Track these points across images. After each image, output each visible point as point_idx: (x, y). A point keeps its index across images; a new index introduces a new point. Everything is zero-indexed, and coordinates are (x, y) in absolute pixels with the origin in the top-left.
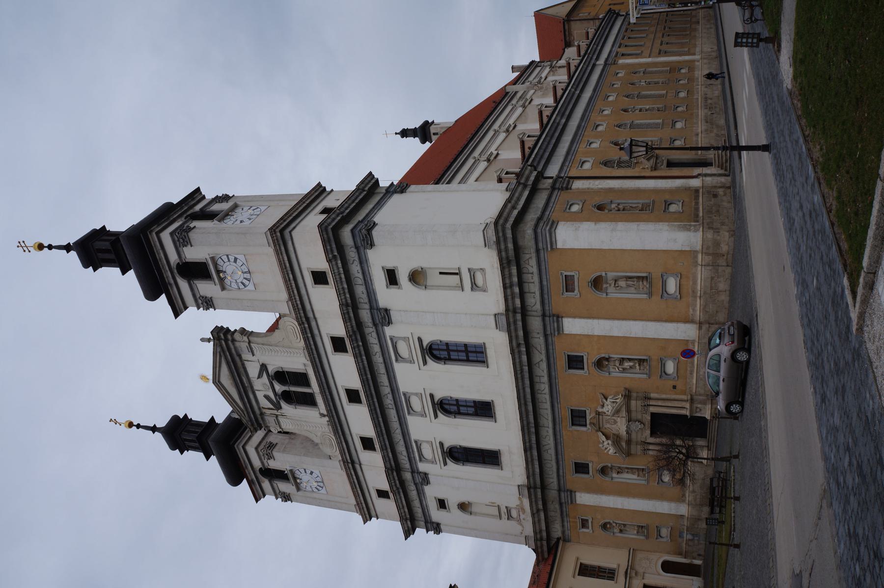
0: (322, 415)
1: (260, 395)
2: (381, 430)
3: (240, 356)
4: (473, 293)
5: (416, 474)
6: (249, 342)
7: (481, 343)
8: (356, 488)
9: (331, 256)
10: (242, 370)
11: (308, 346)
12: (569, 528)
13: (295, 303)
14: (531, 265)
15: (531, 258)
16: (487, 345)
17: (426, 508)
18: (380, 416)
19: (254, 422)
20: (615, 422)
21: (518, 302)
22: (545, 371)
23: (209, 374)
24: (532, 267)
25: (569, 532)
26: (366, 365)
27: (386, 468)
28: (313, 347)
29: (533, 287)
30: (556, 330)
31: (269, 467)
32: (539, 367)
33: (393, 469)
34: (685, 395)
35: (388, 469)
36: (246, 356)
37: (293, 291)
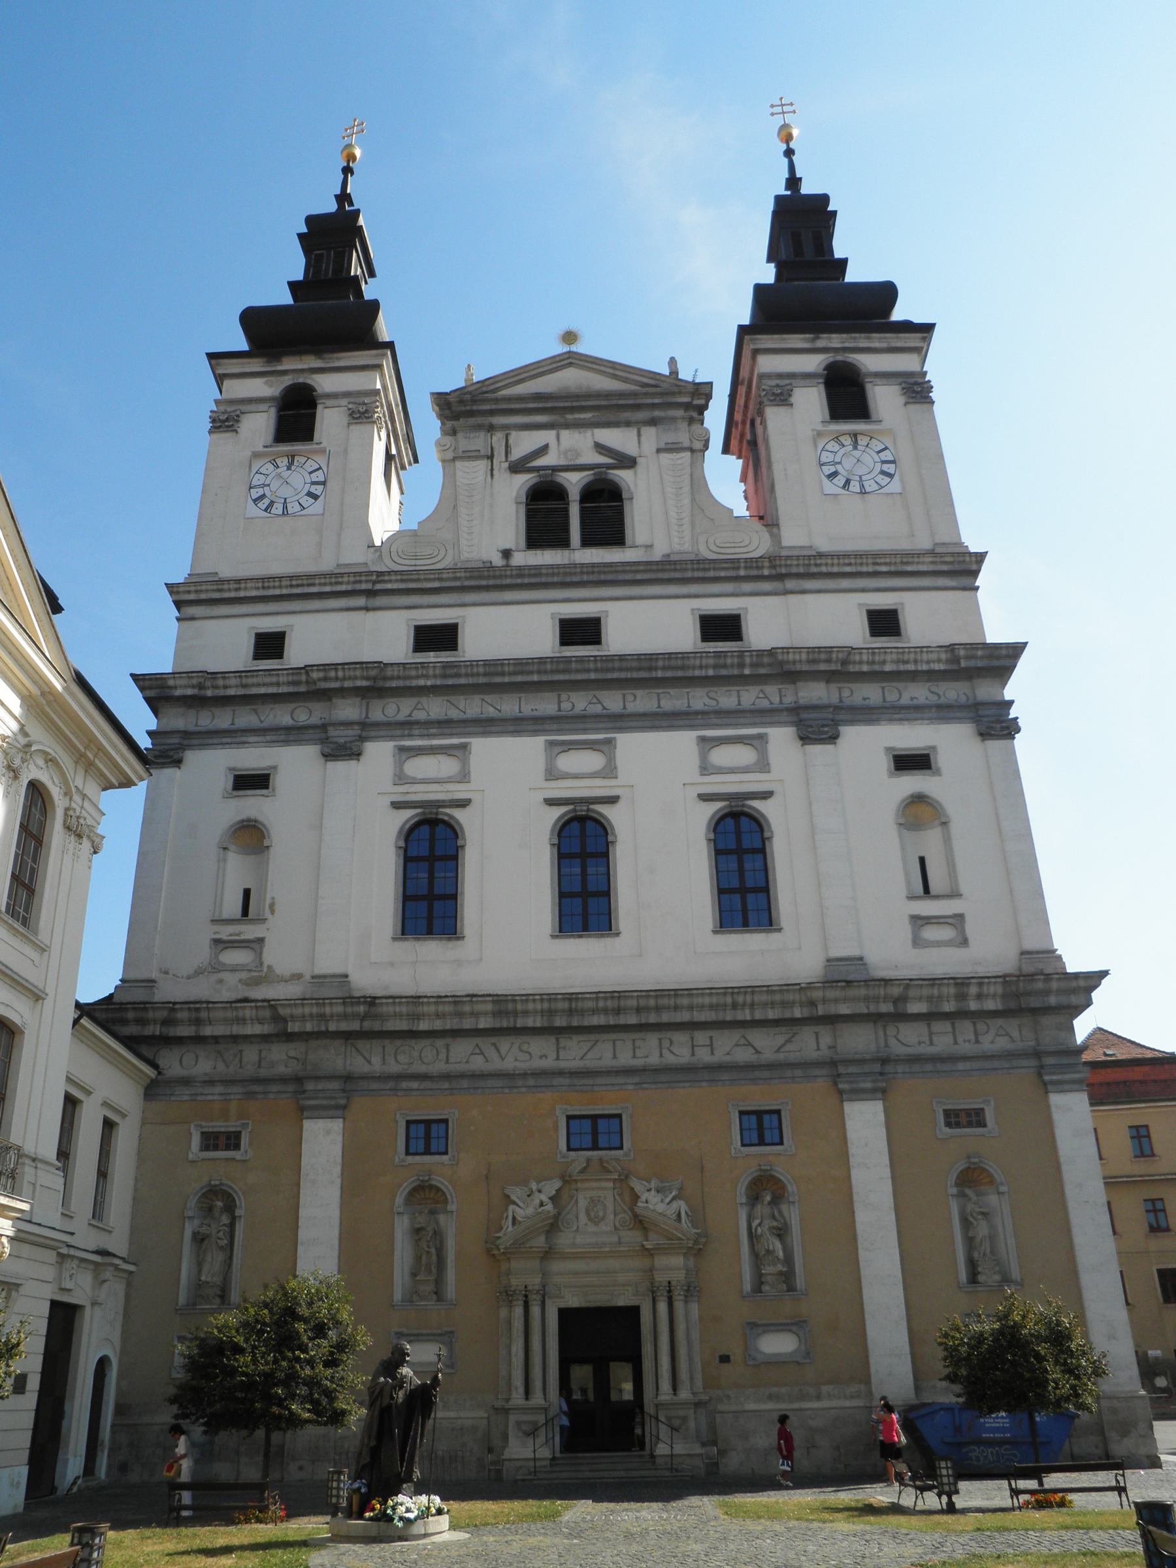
1: (547, 436)
2: (503, 674)
3: (653, 422)
4: (907, 920)
5: (359, 732)
7: (779, 924)
8: (291, 586)
9: (962, 653)
10: (610, 416)
11: (700, 563)
12: (199, 1098)
13: (823, 561)
14: (995, 1039)
15: (1013, 1041)
16: (775, 936)
17: (237, 740)
18: (545, 678)
19: (468, 408)
20: (596, 1220)
21: (914, 1008)
22: (727, 1058)
23: (581, 348)
24: (992, 1042)
25: (186, 1098)
26: (690, 673)
27: (384, 664)
28: (711, 574)
29: (943, 1040)
30: (854, 1086)
31: (320, 408)
32: (737, 1045)
34: (704, 1388)
35: (382, 670)
36: (651, 435)
37: (850, 564)
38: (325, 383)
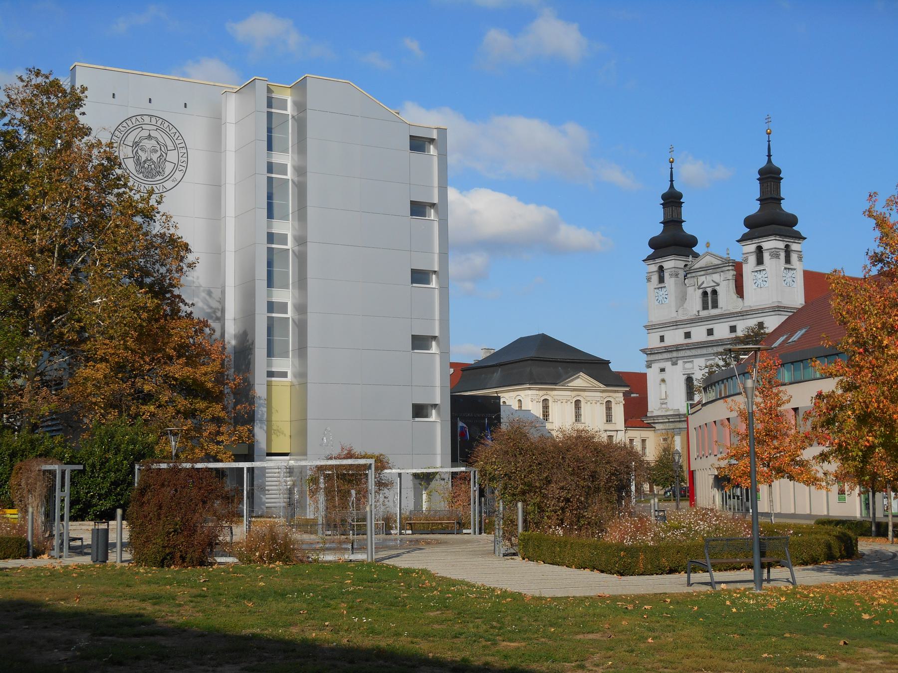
0: (698, 312)
33: (677, 348)
38: (666, 265)
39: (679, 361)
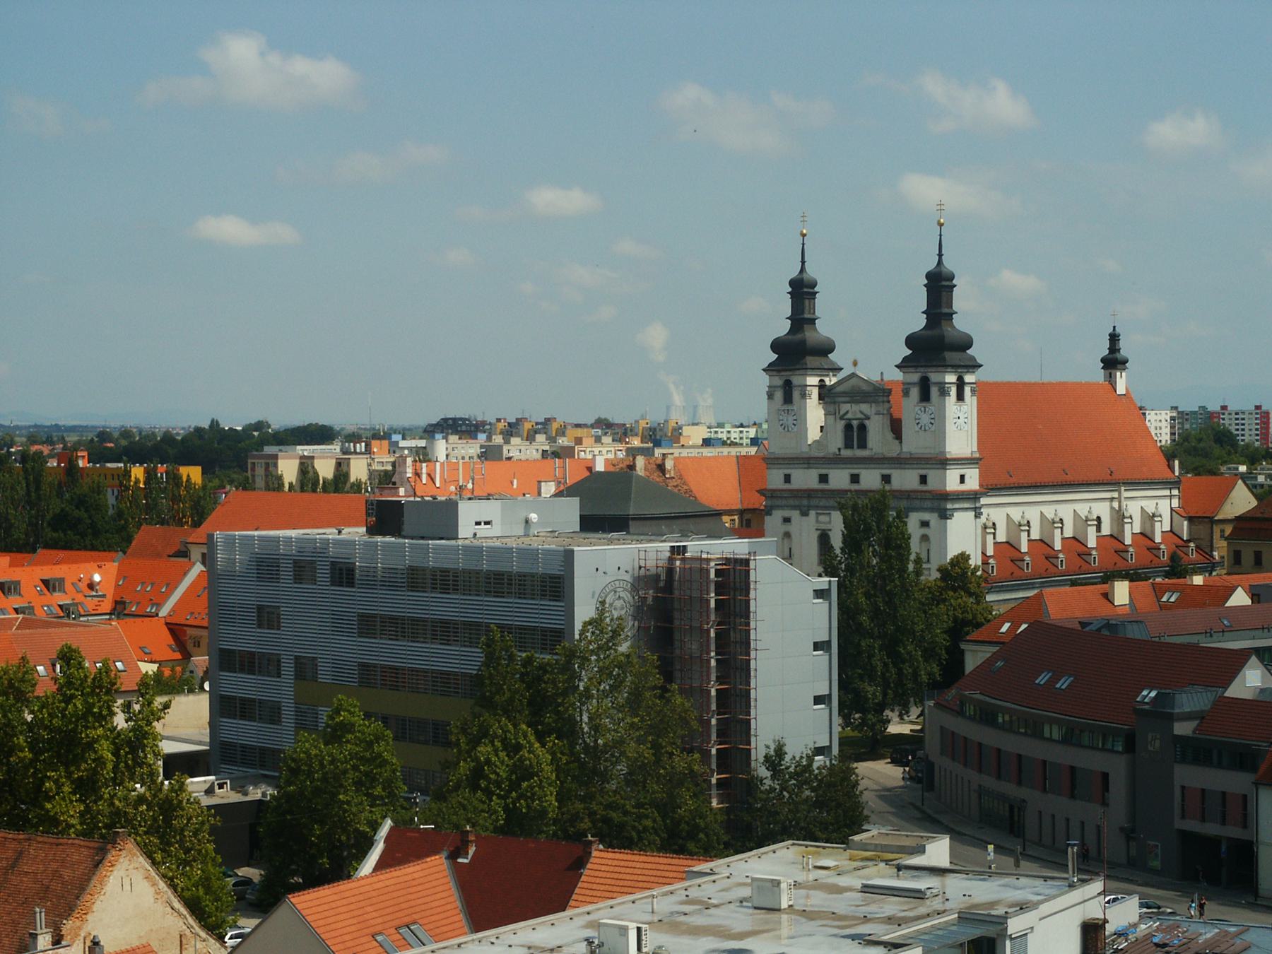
0: (839, 449)
6: (883, 414)
33: (809, 494)
39: (811, 512)
